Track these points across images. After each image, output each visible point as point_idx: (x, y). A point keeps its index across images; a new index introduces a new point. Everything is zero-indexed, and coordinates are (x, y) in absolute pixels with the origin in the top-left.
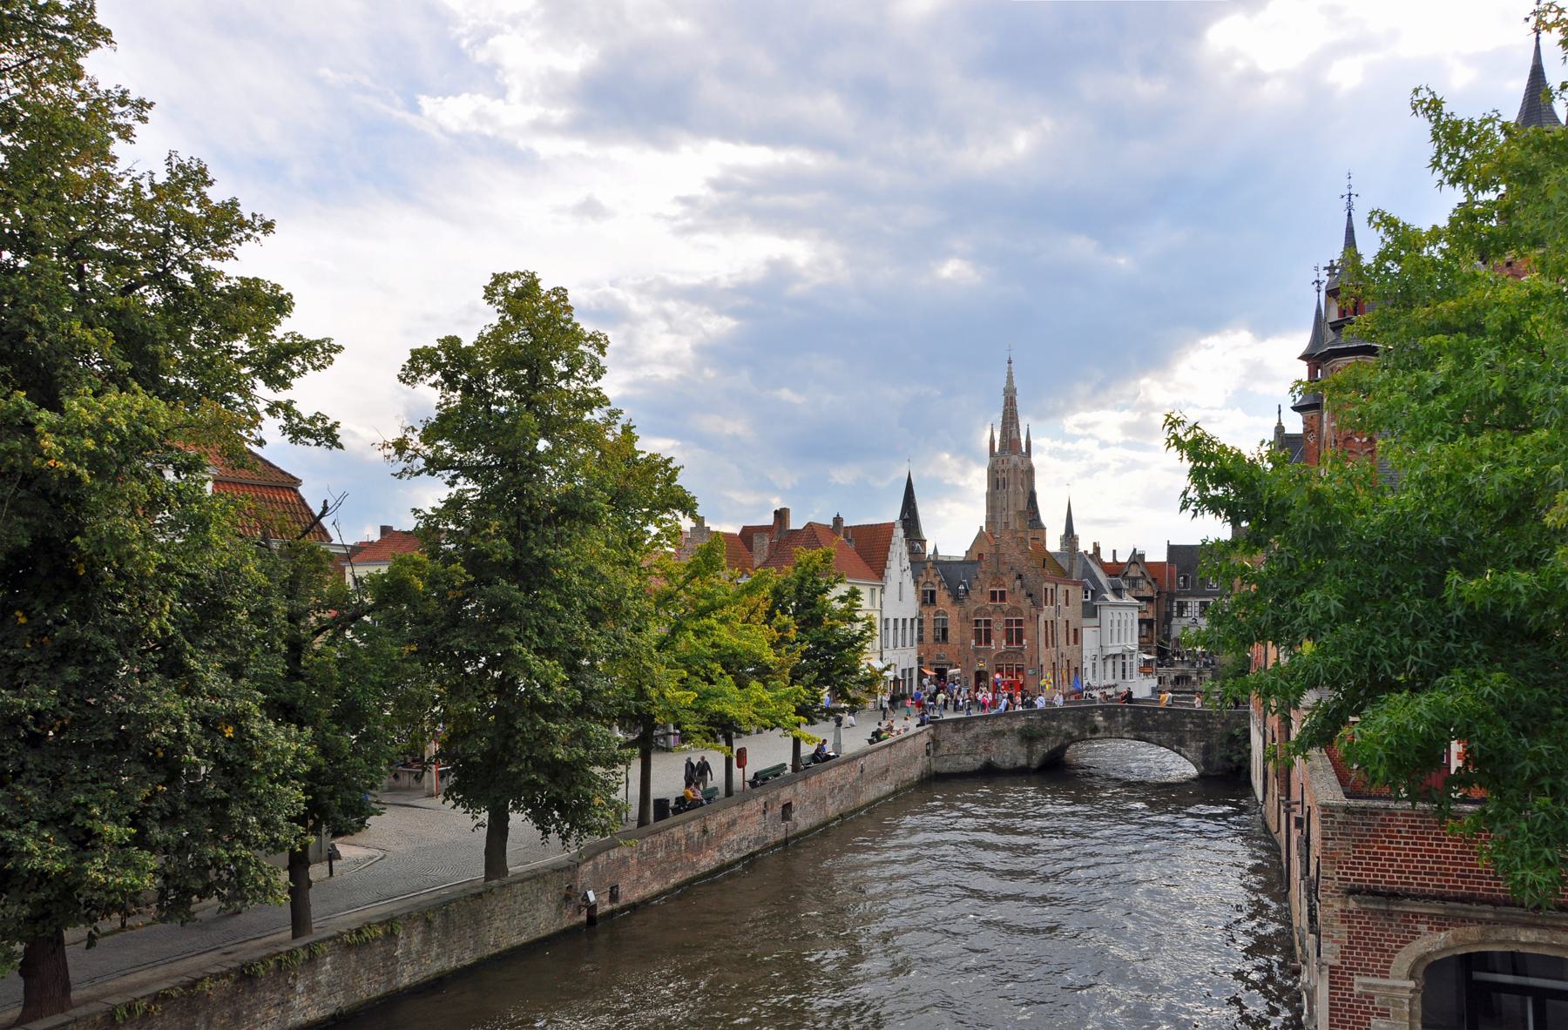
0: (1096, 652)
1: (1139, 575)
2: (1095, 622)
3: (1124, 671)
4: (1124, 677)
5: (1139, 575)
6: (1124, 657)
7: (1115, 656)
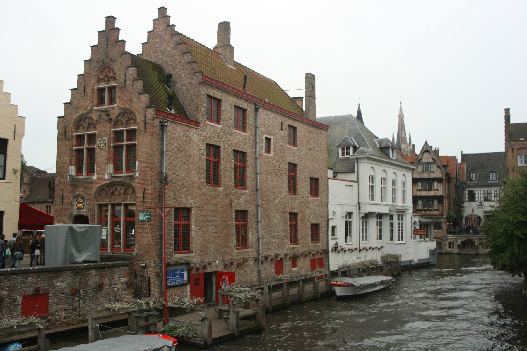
0: (354, 209)
1: (431, 161)
2: (353, 177)
3: (392, 231)
4: (392, 239)
5: (431, 161)
6: (391, 217)
7: (380, 216)
